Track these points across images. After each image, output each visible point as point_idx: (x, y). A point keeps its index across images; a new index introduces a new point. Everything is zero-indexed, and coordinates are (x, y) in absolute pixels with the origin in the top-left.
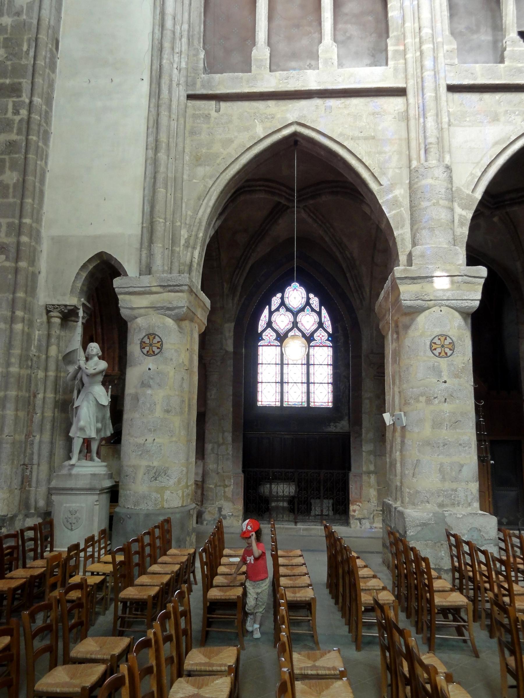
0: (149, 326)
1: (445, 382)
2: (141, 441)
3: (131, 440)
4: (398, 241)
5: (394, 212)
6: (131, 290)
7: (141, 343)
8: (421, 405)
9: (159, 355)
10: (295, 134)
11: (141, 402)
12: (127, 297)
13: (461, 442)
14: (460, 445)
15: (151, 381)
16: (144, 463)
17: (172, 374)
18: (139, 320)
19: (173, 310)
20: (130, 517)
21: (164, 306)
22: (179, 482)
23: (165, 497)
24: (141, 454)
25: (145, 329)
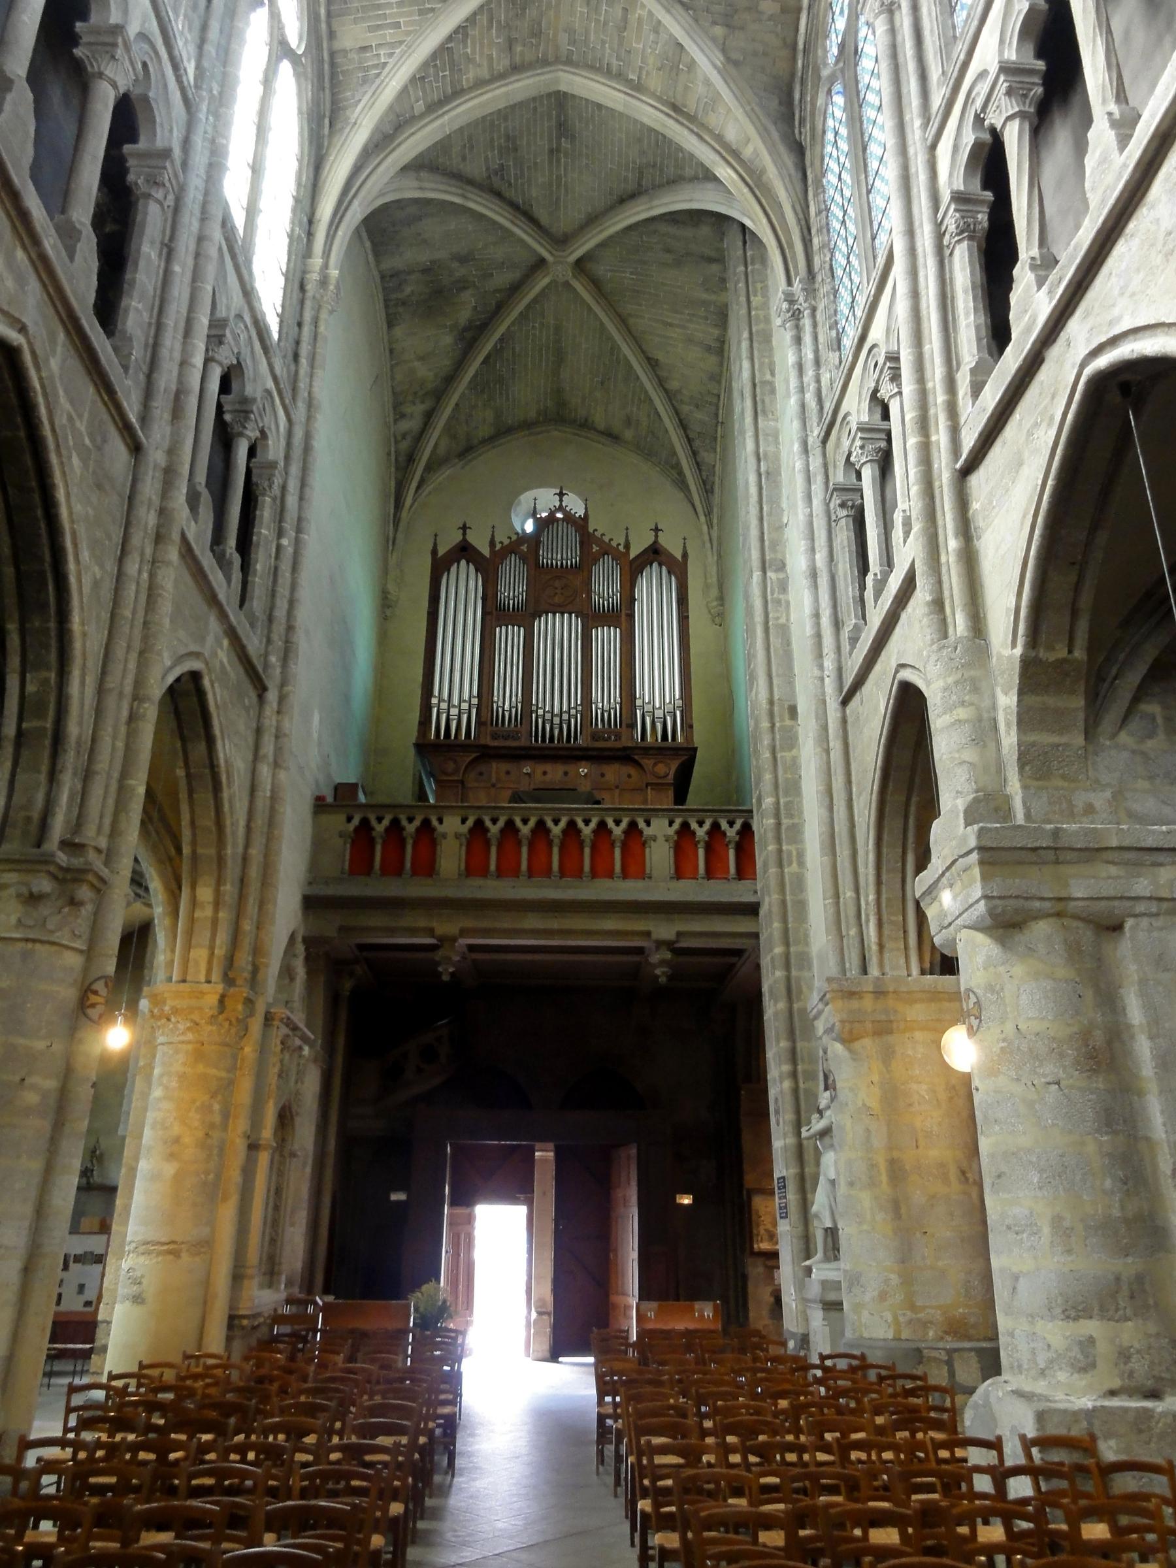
13: (1008, 1221)
14: (1009, 1227)
17: (848, 1123)
22: (883, 1296)
23: (863, 1321)
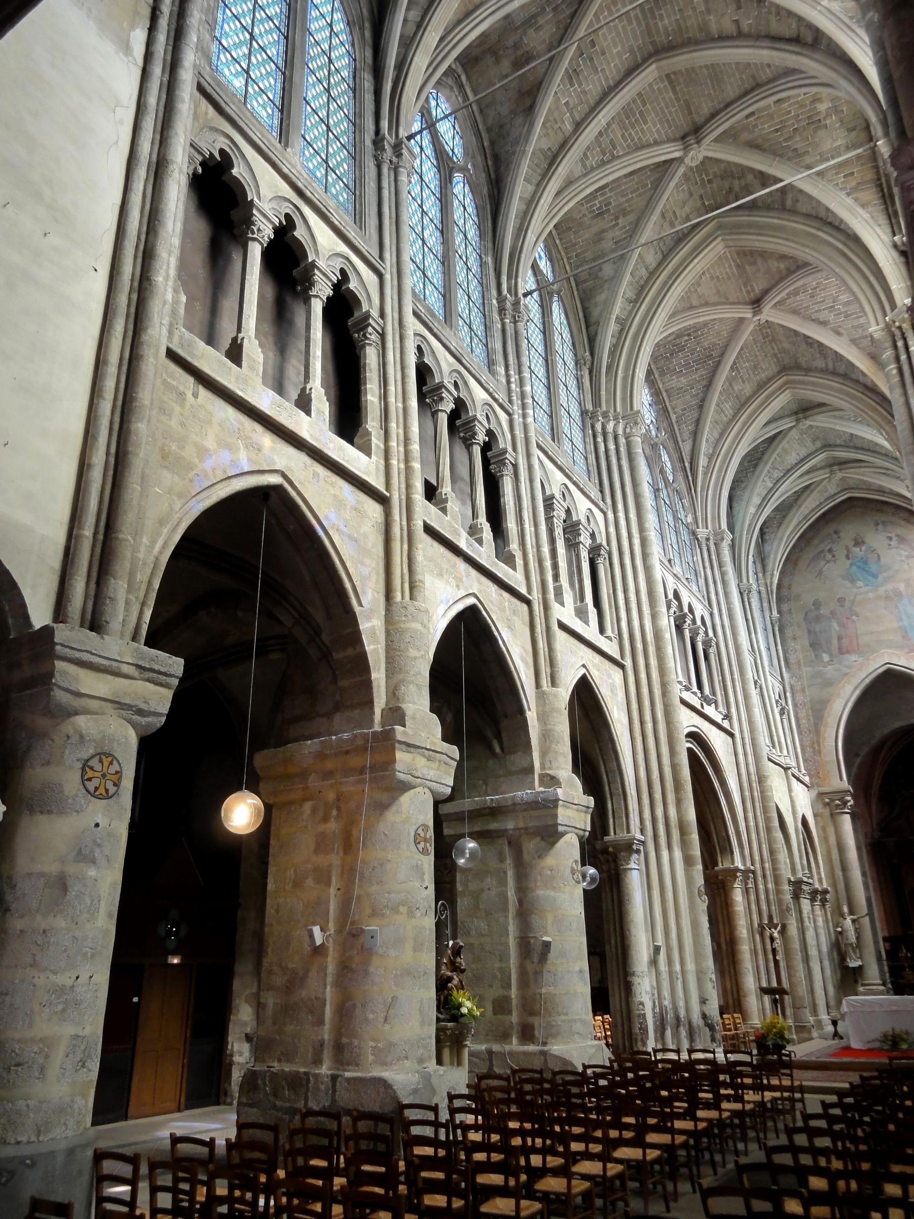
0: (104, 737)
1: (426, 888)
2: (65, 979)
3: (41, 980)
4: (375, 685)
5: (372, 647)
6: (86, 657)
7: (83, 769)
8: (401, 919)
9: (114, 799)
10: (278, 488)
11: (72, 893)
12: (72, 669)
15: (97, 850)
16: (69, 1030)
18: (81, 721)
19: (144, 716)
20: (33, 1165)
21: (136, 706)
24: (64, 1010)
25: (94, 741)
